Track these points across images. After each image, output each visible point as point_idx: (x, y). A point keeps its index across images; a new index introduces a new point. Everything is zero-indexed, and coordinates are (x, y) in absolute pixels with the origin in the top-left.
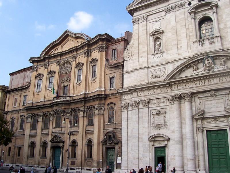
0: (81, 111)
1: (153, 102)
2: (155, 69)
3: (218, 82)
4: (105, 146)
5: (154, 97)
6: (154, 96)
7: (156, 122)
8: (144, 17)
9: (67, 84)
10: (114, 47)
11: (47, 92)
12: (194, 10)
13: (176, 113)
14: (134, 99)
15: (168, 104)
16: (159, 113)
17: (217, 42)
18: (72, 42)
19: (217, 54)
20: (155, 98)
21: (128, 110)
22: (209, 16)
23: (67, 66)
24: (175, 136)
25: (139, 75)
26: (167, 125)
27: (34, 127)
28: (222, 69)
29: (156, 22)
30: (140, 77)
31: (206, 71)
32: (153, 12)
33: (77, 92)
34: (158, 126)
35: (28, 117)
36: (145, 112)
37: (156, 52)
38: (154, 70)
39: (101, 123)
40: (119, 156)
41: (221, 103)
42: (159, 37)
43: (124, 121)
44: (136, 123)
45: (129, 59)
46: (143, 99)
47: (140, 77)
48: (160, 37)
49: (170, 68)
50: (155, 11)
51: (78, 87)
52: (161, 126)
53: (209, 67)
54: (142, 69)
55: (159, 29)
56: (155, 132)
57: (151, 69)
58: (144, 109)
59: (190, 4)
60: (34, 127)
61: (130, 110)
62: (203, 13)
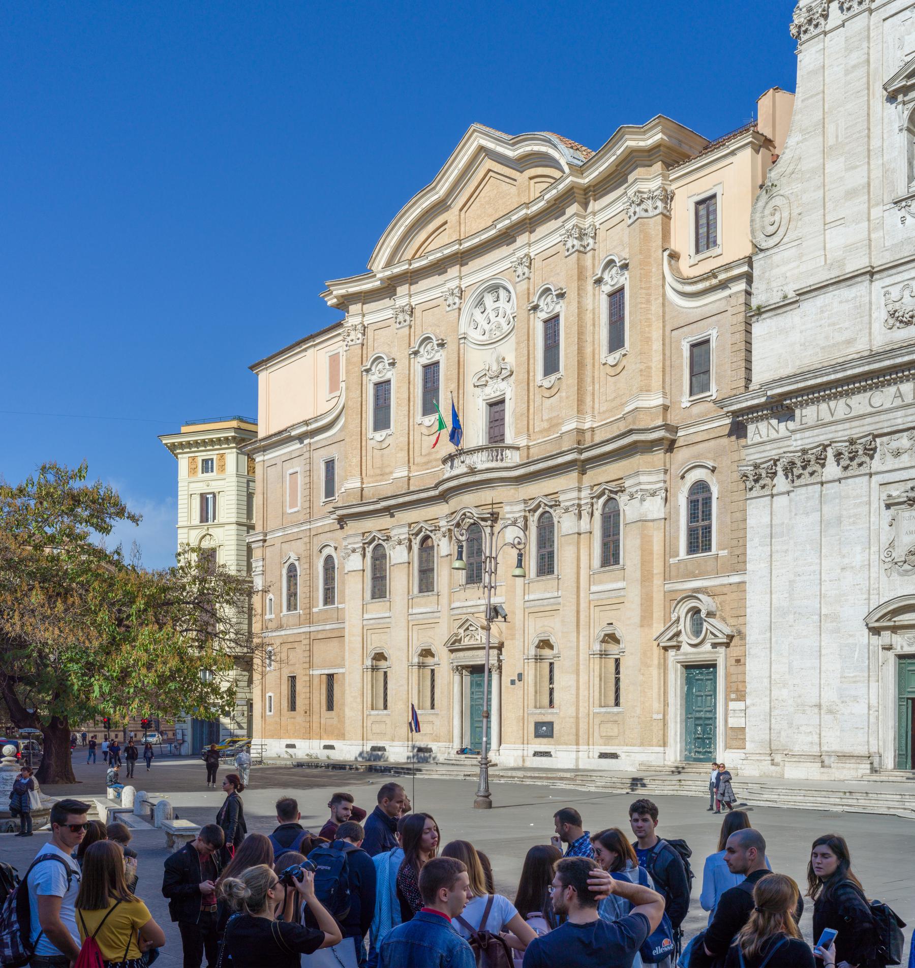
0: (567, 510)
1: (894, 445)
6: (900, 413)
9: (498, 393)
11: (417, 438)
14: (798, 436)
18: (505, 187)
20: (901, 427)
21: (775, 491)
23: (497, 304)
25: (826, 314)
30: (834, 324)
33: (545, 425)
38: (902, 285)
39: (655, 556)
44: (808, 547)
46: (842, 433)
47: (834, 324)
51: (548, 402)
54: (843, 284)
57: (888, 281)
58: (850, 480)
61: (784, 490)
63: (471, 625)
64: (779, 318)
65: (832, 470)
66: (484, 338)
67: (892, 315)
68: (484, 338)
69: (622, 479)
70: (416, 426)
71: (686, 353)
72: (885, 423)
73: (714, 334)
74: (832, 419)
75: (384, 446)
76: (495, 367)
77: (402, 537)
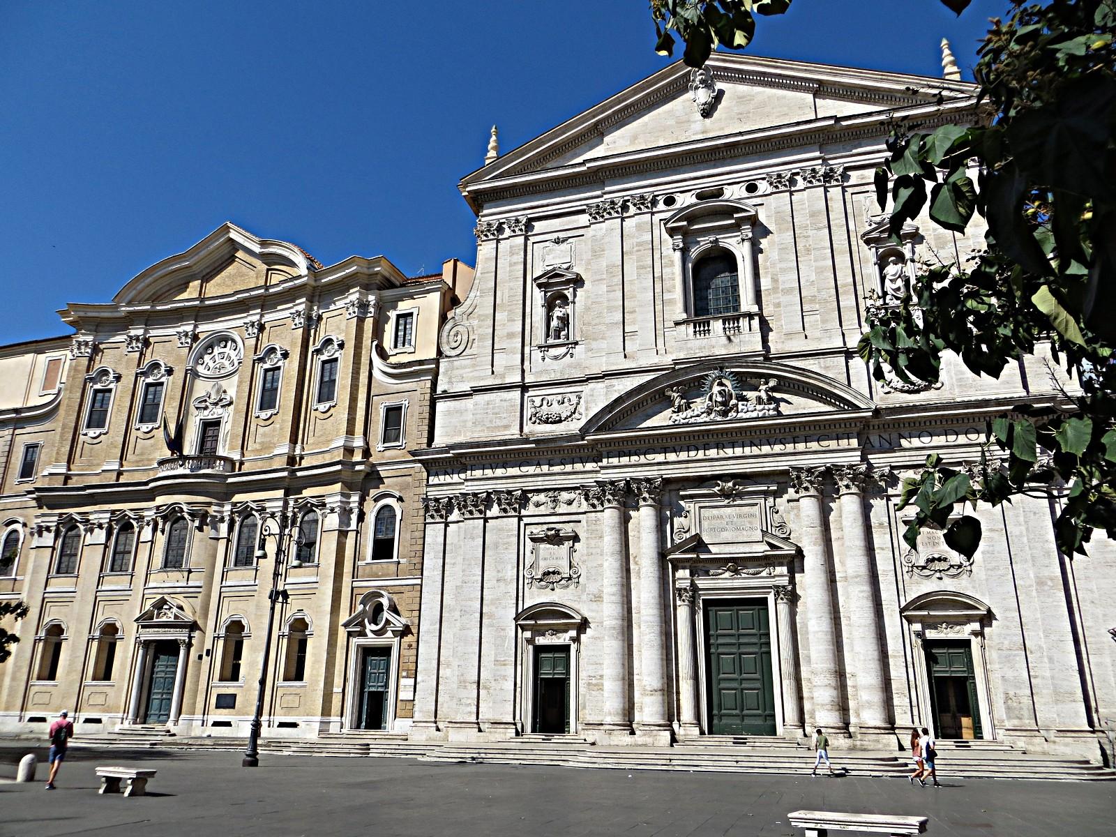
4: (355, 641)
5: (540, 483)
7: (543, 566)
9: (215, 416)
10: (404, 306)
13: (610, 540)
14: (469, 483)
15: (585, 506)
16: (555, 539)
17: (750, 330)
19: (748, 367)
22: (726, 246)
24: (604, 615)
25: (491, 406)
26: (579, 577)
27: (65, 563)
28: (761, 414)
29: (558, 243)
30: (496, 414)
33: (257, 446)
35: (40, 531)
36: (504, 528)
37: (551, 341)
38: (541, 398)
40: (404, 674)
42: (566, 292)
45: (457, 352)
47: (496, 414)
48: (569, 295)
49: (598, 398)
51: (261, 430)
52: (557, 577)
53: (723, 404)
55: (565, 266)
56: (535, 597)
59: (670, 201)
60: (65, 563)
61: (455, 520)
64: (456, 402)
66: (209, 373)
68: (209, 373)
69: (323, 496)
70: (133, 430)
72: (530, 484)
74: (493, 476)
75: (95, 441)
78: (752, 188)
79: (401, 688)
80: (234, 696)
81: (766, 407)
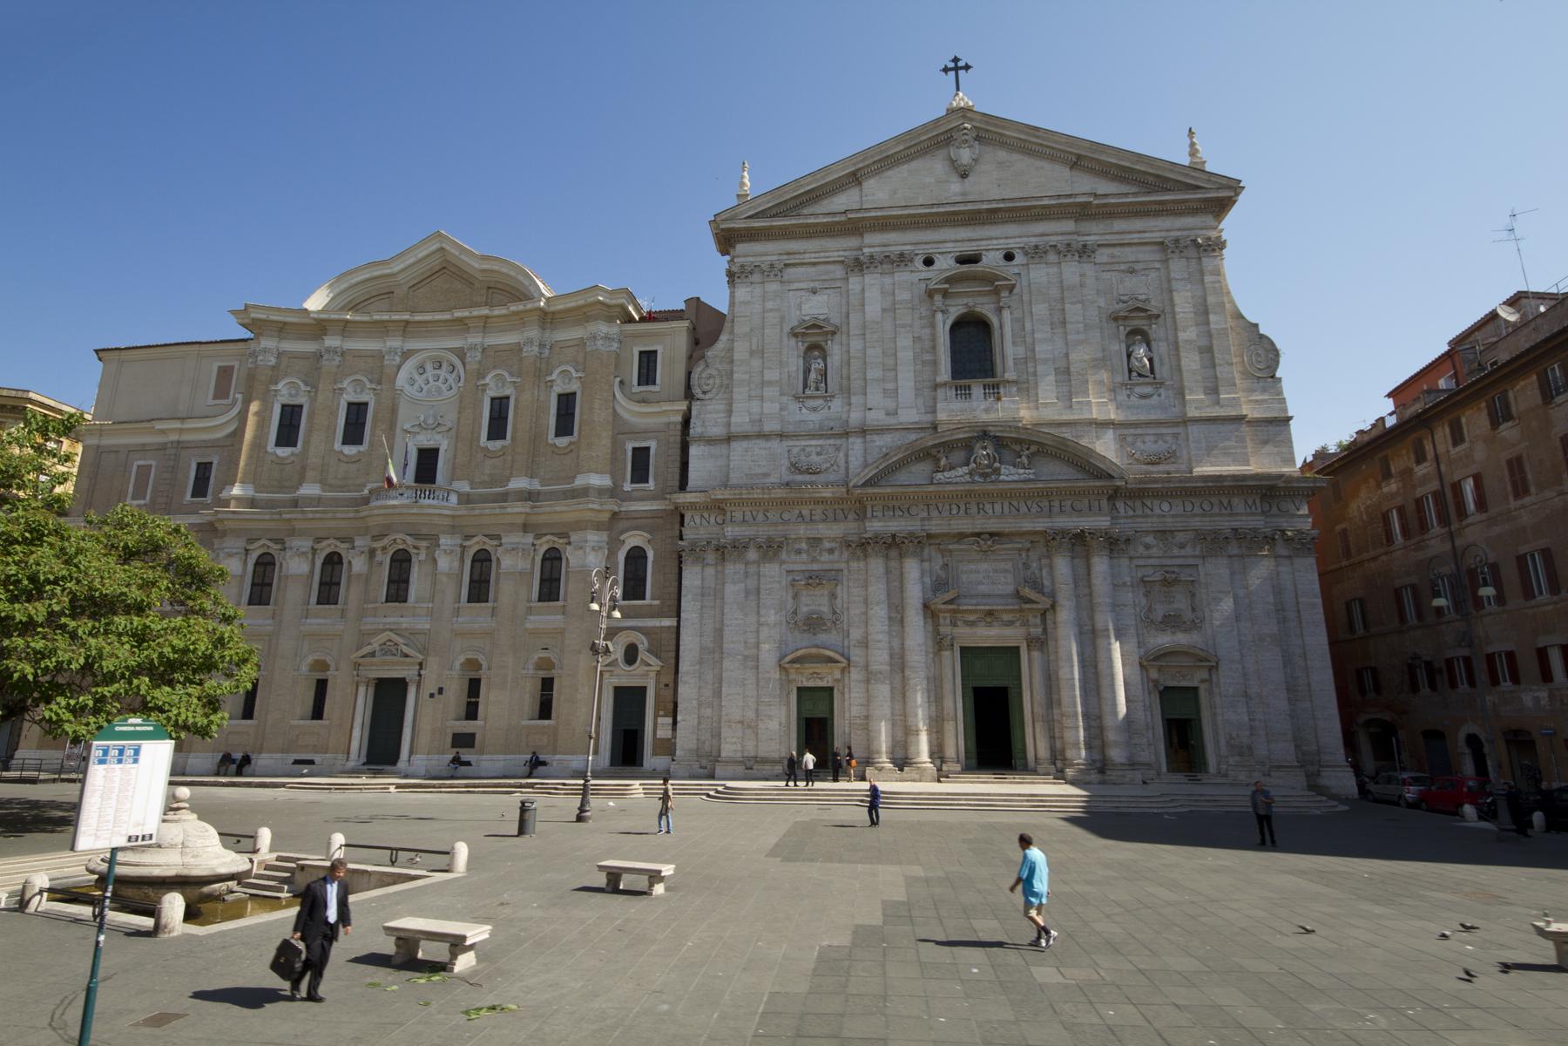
1: (797, 546)
2: (804, 443)
3: (1006, 510)
8: (772, 266)
9: (431, 443)
12: (946, 286)
13: (878, 590)
22: (984, 311)
28: (1022, 477)
29: (815, 293)
31: (977, 478)
32: (808, 258)
33: (486, 478)
34: (813, 624)
40: (661, 713)
41: (1006, 571)
43: (690, 597)
50: (813, 255)
59: (929, 262)
62: (970, 301)
63: (390, 640)
65: (752, 555)
67: (793, 465)
71: (630, 454)
73: (653, 445)
76: (430, 421)
77: (304, 550)
78: (1009, 257)
79: (659, 727)
80: (473, 736)
81: (1027, 471)
